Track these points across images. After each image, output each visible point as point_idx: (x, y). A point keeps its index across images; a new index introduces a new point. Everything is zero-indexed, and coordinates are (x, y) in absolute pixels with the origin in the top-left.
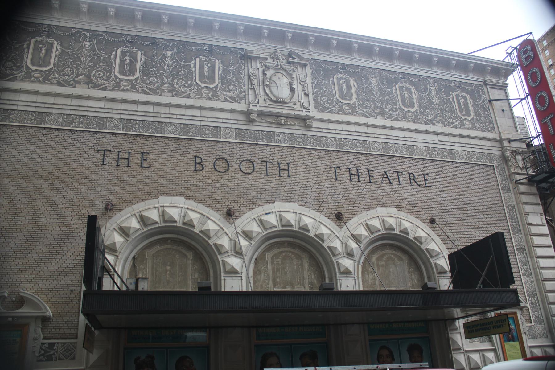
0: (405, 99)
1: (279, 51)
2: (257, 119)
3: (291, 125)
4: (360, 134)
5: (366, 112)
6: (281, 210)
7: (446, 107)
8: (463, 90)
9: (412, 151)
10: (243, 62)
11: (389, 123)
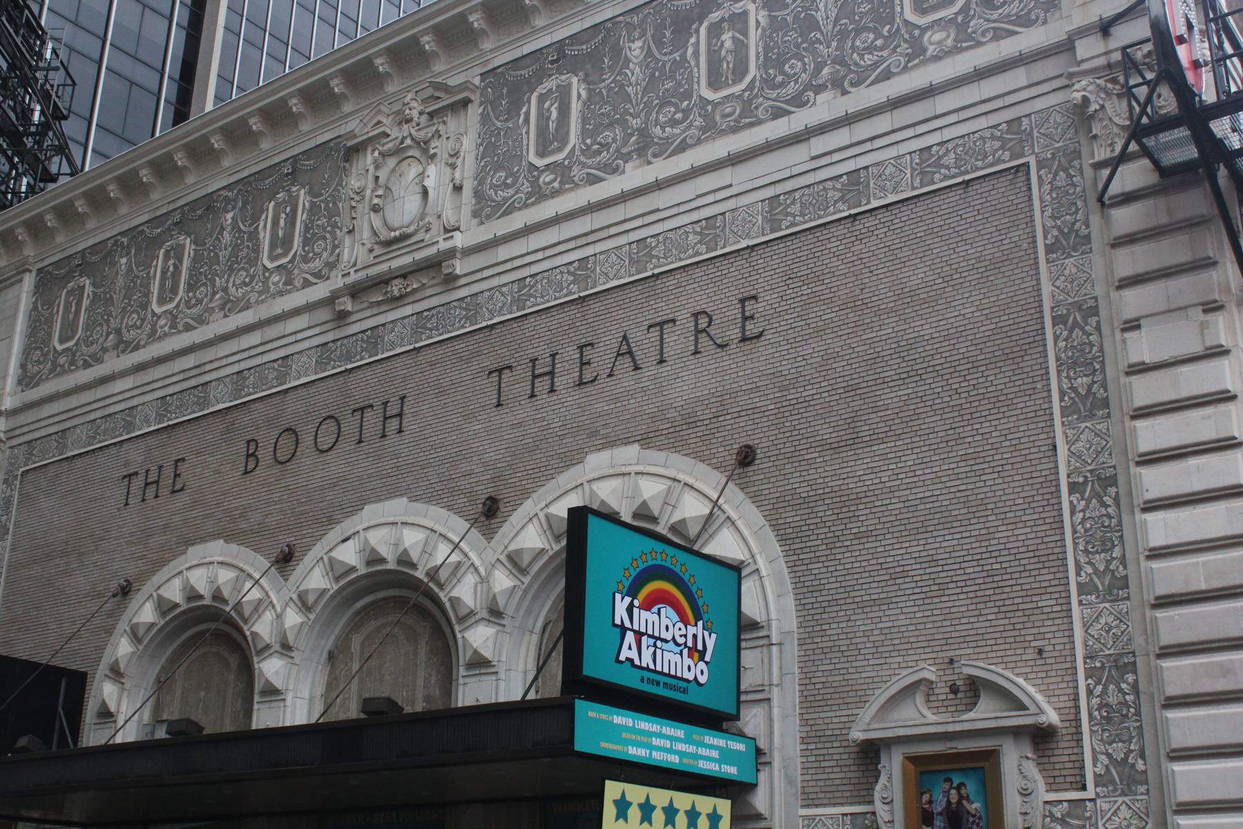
0: (720, 61)
2: (349, 308)
7: (862, 15)
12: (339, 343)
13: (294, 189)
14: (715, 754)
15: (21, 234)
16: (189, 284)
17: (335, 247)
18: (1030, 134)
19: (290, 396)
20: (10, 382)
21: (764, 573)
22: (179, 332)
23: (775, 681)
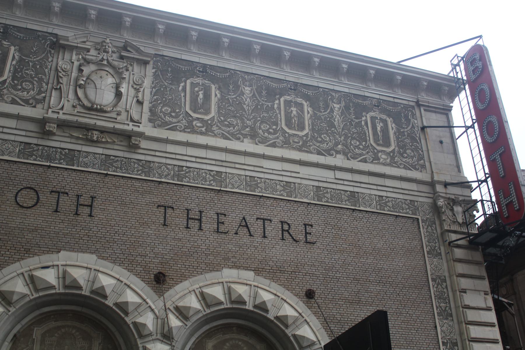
1: (108, 41)
2: (55, 131)
3: (107, 142)
5: (228, 132)
6: (68, 263)
7: (354, 133)
8: (384, 111)
9: (291, 191)
10: (53, 51)
11: (260, 149)
18: (418, 208)
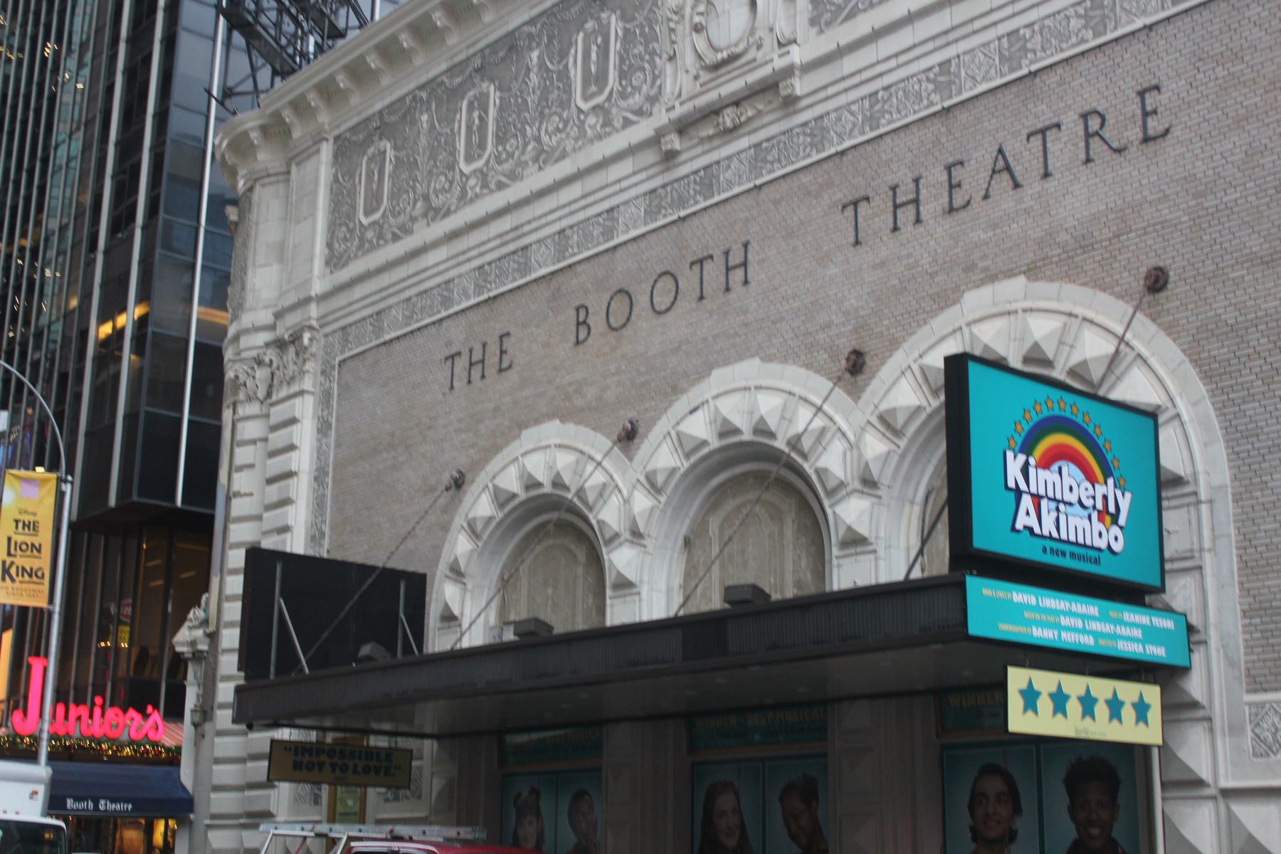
2: (677, 146)
4: (930, 46)
9: (1104, 17)
12: (669, 189)
13: (604, 15)
14: (1137, 633)
15: (313, 99)
16: (498, 137)
17: (655, 78)
19: (619, 253)
20: (318, 264)
21: (1185, 417)
22: (492, 191)
23: (1207, 544)
